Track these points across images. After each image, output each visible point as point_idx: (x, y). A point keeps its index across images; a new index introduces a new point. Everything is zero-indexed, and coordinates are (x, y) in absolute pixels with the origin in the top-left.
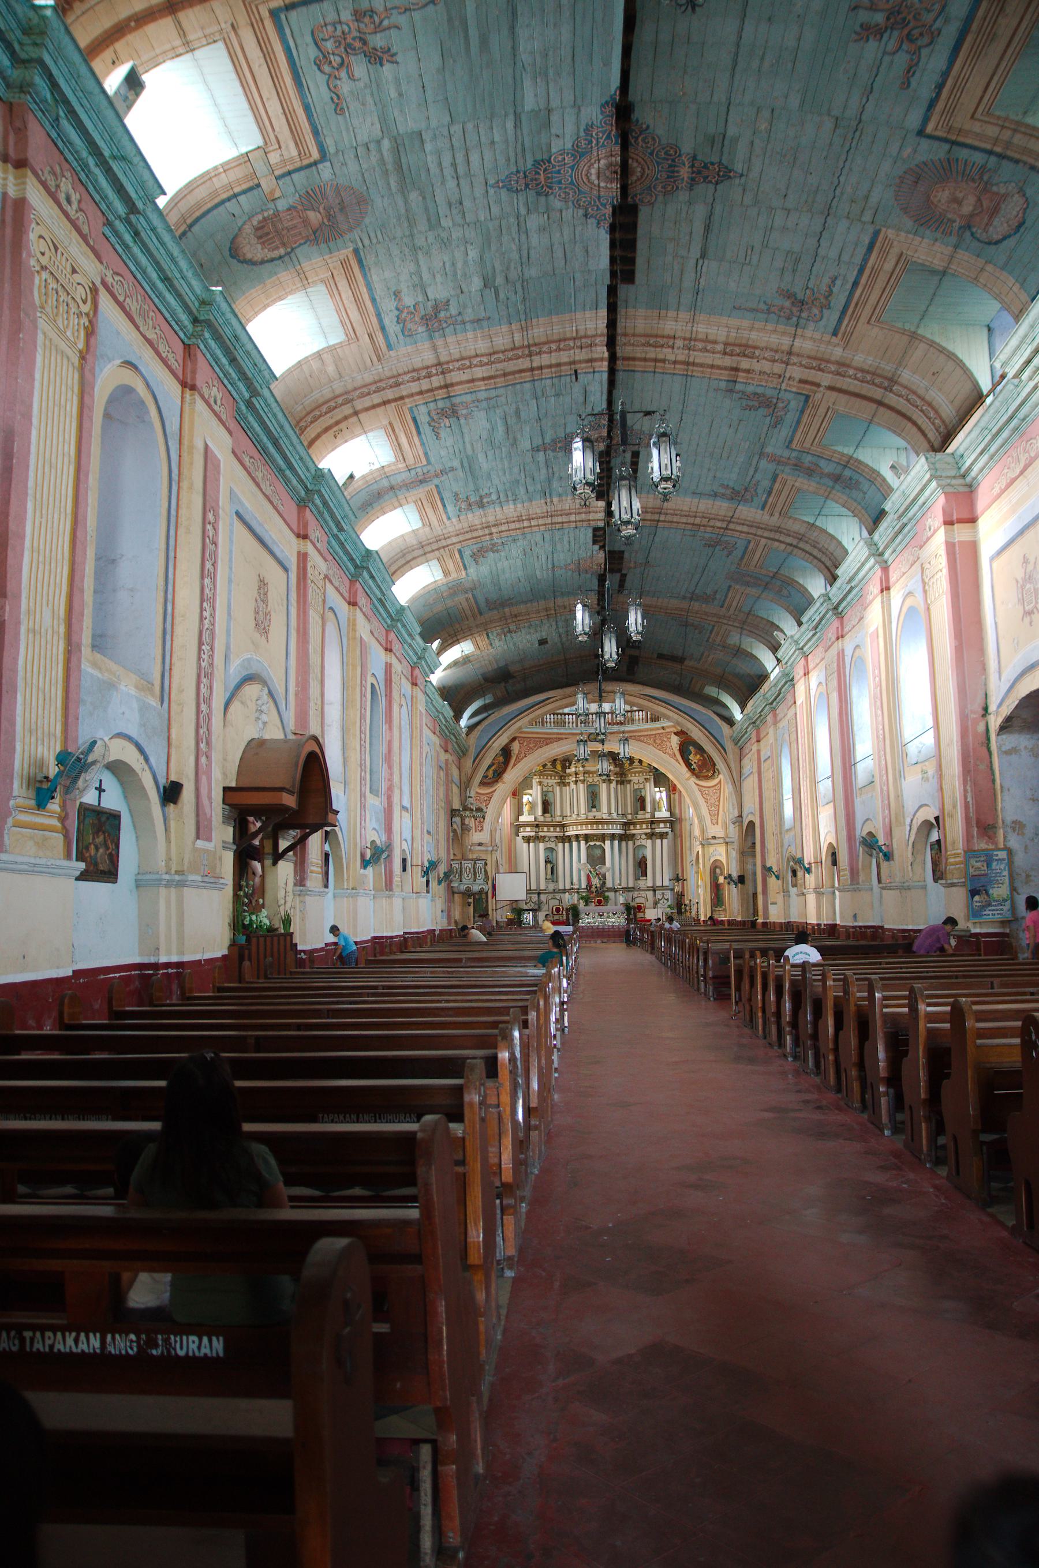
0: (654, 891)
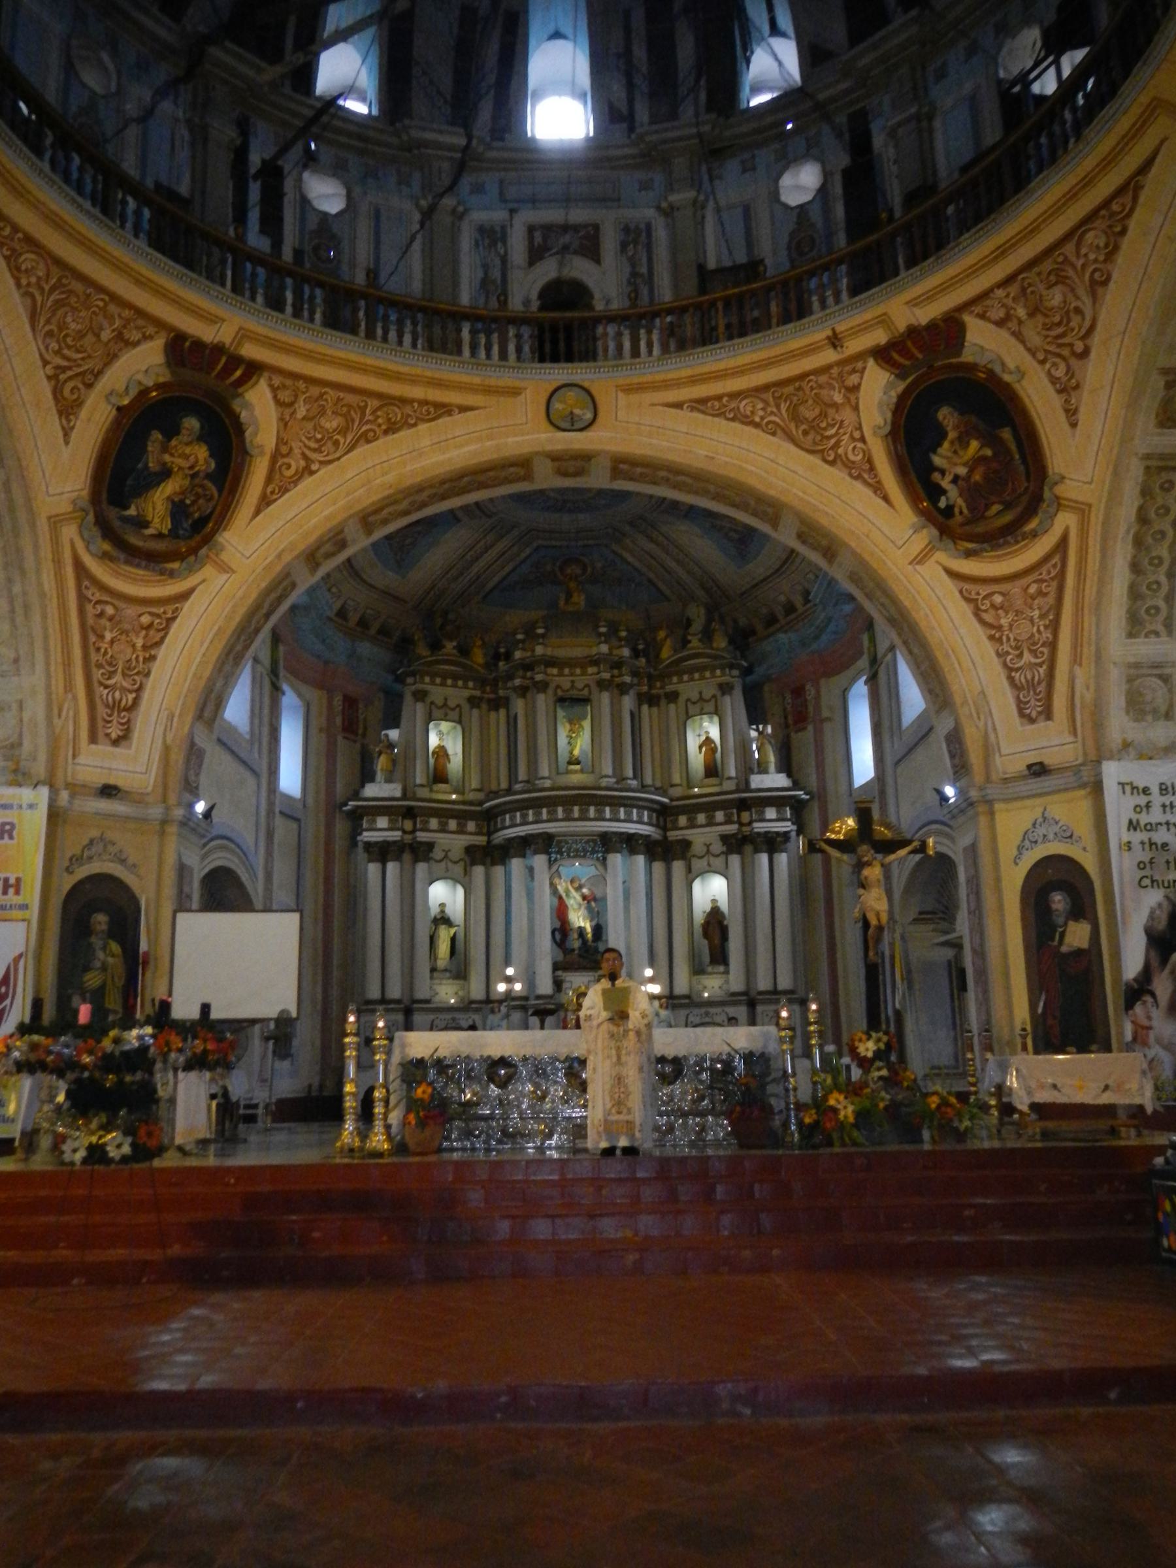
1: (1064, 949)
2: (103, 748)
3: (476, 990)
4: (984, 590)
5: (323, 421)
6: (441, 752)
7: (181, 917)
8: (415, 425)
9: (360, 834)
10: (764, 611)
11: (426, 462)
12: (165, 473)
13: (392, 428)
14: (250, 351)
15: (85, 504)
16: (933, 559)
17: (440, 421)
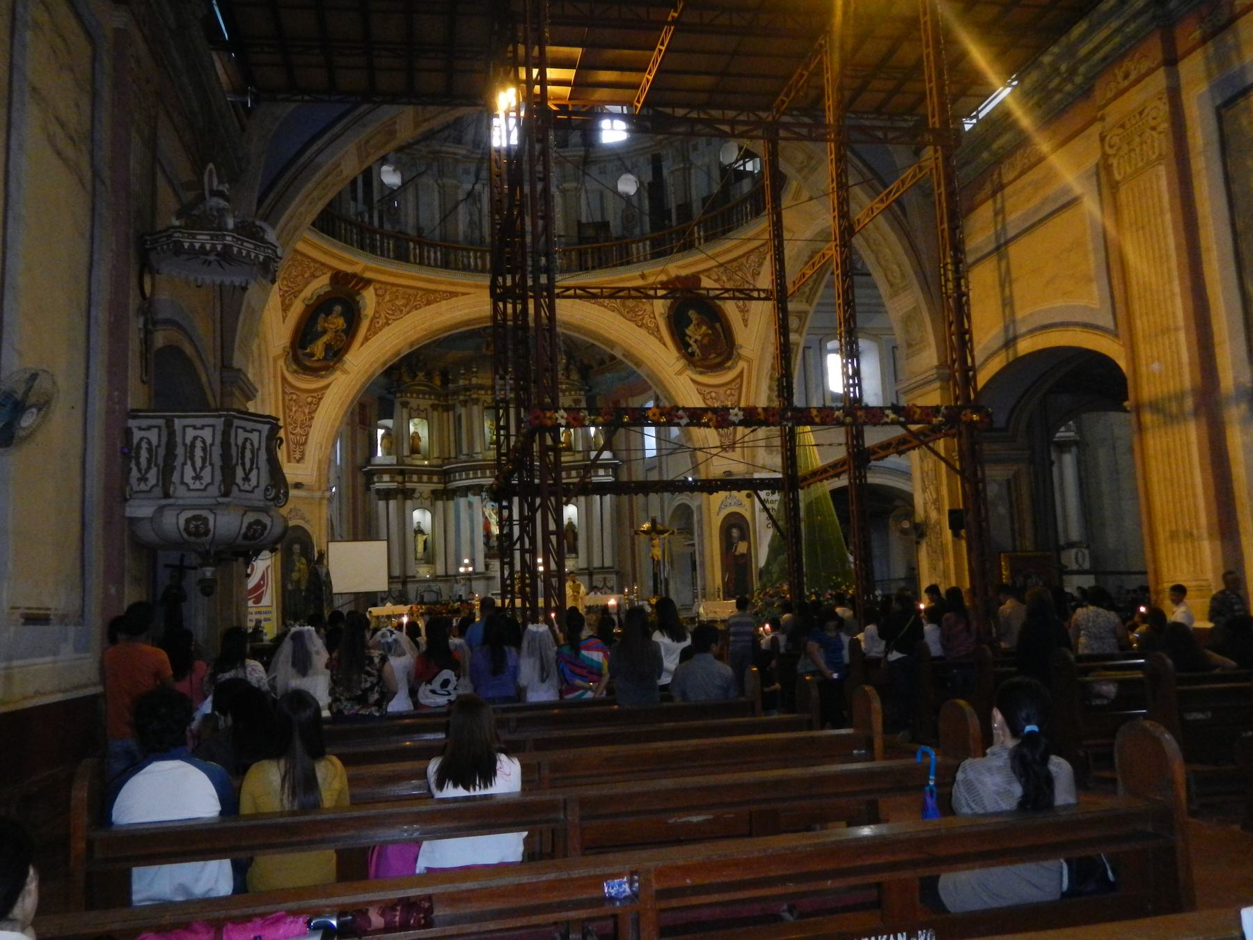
0: (591, 575)
1: (737, 553)
2: (293, 464)
3: (440, 570)
4: (708, 390)
6: (416, 433)
7: (330, 544)
9: (374, 483)
10: (598, 357)
11: (442, 318)
12: (325, 332)
13: (429, 303)
14: (368, 275)
15: (288, 349)
16: (684, 376)
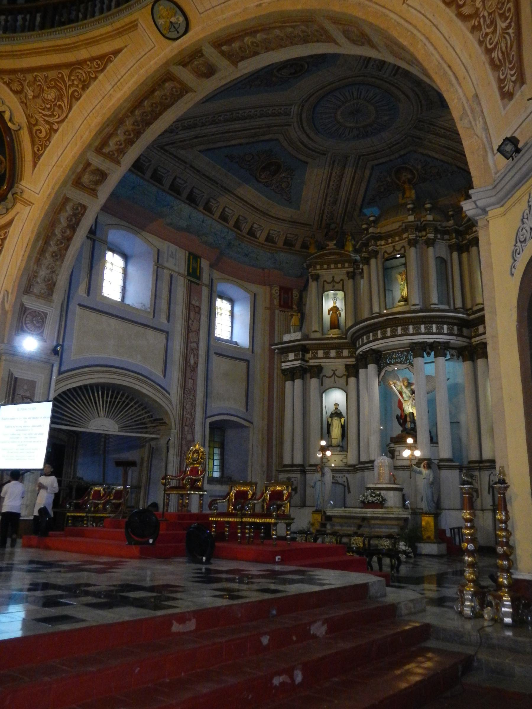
5: (46, 96)
6: (335, 310)
8: (96, 78)
17: (108, 68)
